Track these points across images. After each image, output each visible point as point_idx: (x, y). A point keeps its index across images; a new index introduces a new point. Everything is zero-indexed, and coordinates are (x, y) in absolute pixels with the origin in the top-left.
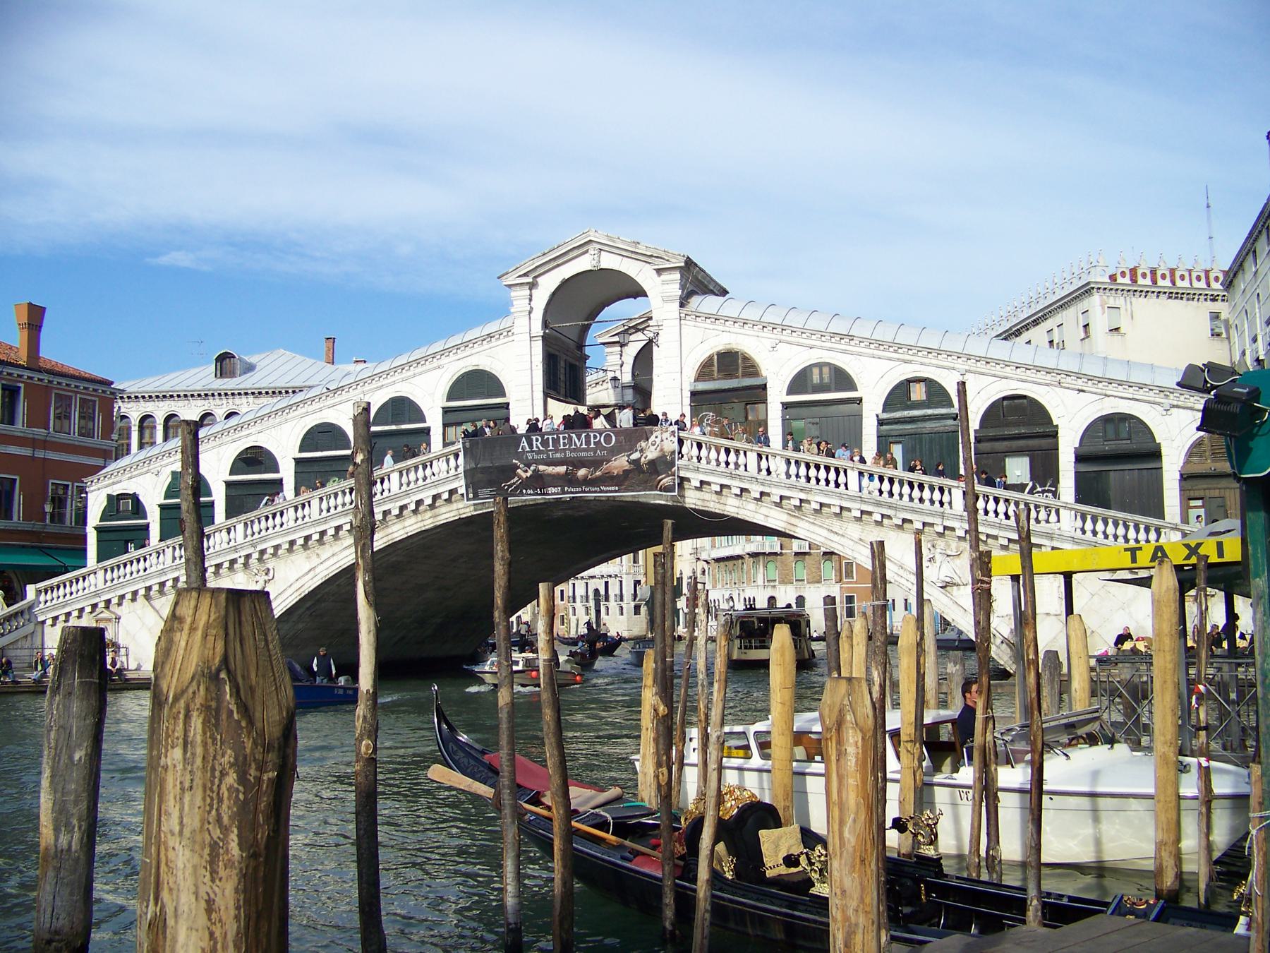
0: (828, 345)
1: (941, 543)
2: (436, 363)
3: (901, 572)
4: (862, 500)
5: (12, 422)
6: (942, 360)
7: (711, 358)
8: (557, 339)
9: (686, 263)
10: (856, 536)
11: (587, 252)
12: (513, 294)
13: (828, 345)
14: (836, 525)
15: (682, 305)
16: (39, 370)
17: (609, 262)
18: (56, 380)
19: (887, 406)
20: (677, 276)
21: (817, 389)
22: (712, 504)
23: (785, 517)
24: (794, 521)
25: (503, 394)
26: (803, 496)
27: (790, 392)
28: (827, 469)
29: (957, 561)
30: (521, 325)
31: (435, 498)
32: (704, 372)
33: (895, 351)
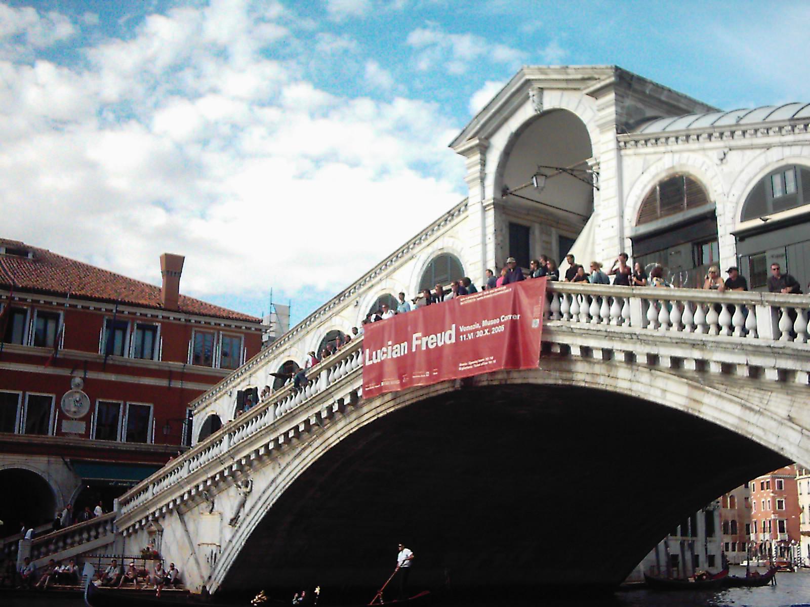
0: (790, 138)
2: (409, 255)
4: (774, 352)
5: (152, 358)
7: (653, 191)
8: (537, 210)
10: (783, 412)
11: (528, 98)
14: (755, 398)
16: (178, 311)
17: (552, 101)
18: (193, 319)
20: (611, 97)
21: (781, 205)
23: (684, 390)
24: (697, 395)
26: (697, 354)
27: (745, 217)
28: (731, 310)
31: (354, 394)
32: (646, 211)
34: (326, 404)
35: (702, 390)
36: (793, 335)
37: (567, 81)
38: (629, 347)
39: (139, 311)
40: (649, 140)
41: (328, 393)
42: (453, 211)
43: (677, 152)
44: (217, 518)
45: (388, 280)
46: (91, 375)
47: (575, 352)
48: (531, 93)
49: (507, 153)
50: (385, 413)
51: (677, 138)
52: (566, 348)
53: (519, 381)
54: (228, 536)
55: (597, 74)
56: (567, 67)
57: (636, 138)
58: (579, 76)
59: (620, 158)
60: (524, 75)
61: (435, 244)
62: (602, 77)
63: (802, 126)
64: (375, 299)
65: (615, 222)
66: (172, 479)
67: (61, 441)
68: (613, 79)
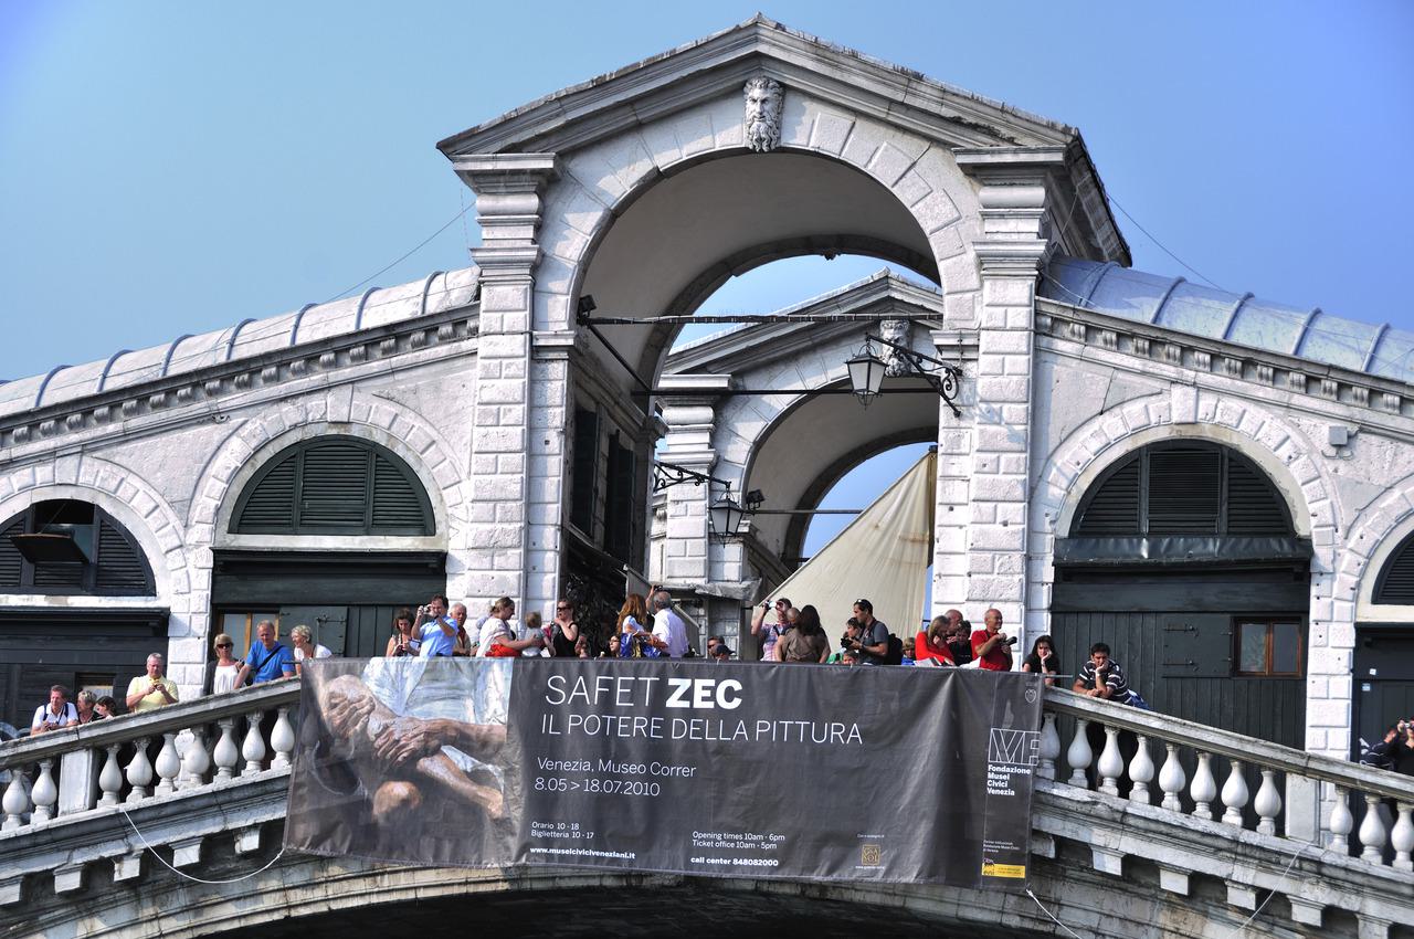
2: (199, 407)
9: (1068, 153)
11: (738, 90)
12: (485, 202)
15: (1042, 287)
20: (1037, 194)
25: (423, 521)
34: (81, 858)
37: (892, 101)
40: (1133, 336)
42: (408, 328)
43: (1208, 389)
45: (87, 459)
48: (756, 92)
49: (613, 217)
50: (323, 908)
51: (1214, 357)
55: (1008, 125)
56: (919, 77)
57: (1093, 321)
59: (1039, 355)
60: (757, 40)
61: (315, 404)
62: (1031, 143)
64: (21, 504)
65: (1016, 512)
68: (1058, 157)
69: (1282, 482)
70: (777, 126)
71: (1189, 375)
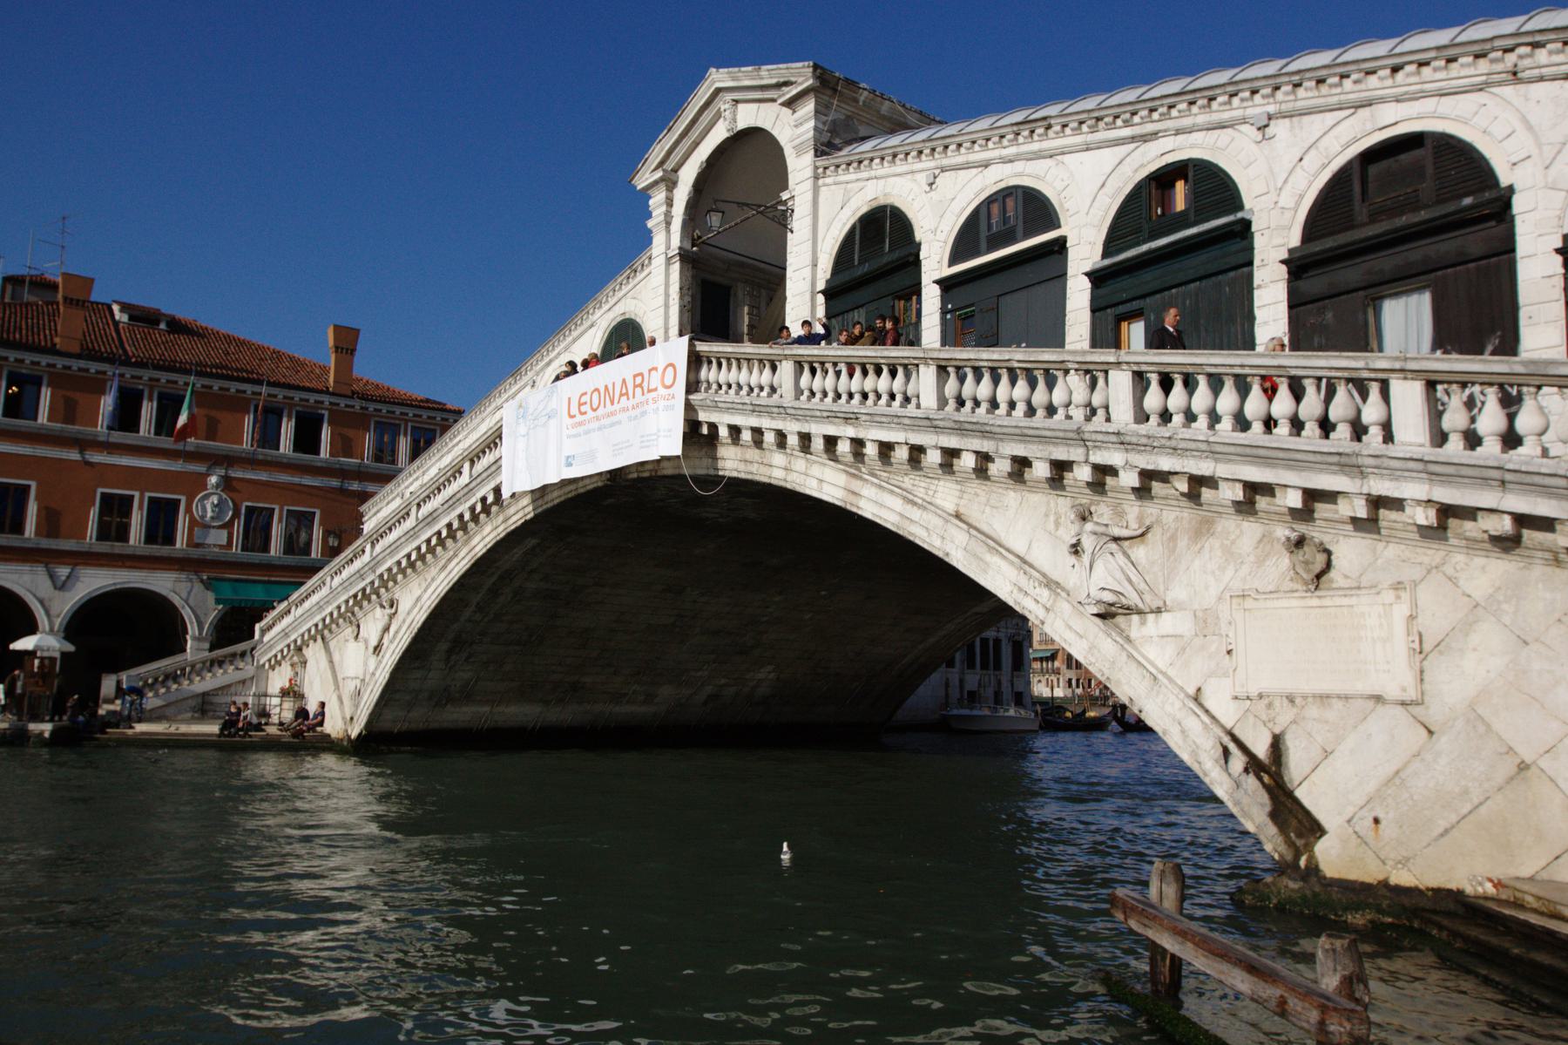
0: (1012, 150)
1: (1103, 511)
3: (1023, 581)
6: (1219, 112)
8: (742, 265)
13: (1012, 150)
15: (819, 153)
18: (372, 407)
19: (1109, 247)
20: (809, 107)
22: (754, 468)
23: (841, 479)
24: (856, 485)
27: (954, 260)
29: (1139, 552)
30: (659, 240)
33: (1127, 123)
35: (861, 478)
36: (961, 403)
38: (779, 424)
39: (297, 395)
41: (469, 490)
44: (361, 645)
46: (237, 473)
47: (723, 432)
52: (713, 427)
53: (669, 472)
54: (372, 668)
58: (774, 81)
59: (816, 191)
63: (1026, 133)
65: (807, 272)
66: (314, 599)
67: (195, 553)
68: (811, 82)
69: (910, 215)
70: (735, 120)
71: (873, 173)
